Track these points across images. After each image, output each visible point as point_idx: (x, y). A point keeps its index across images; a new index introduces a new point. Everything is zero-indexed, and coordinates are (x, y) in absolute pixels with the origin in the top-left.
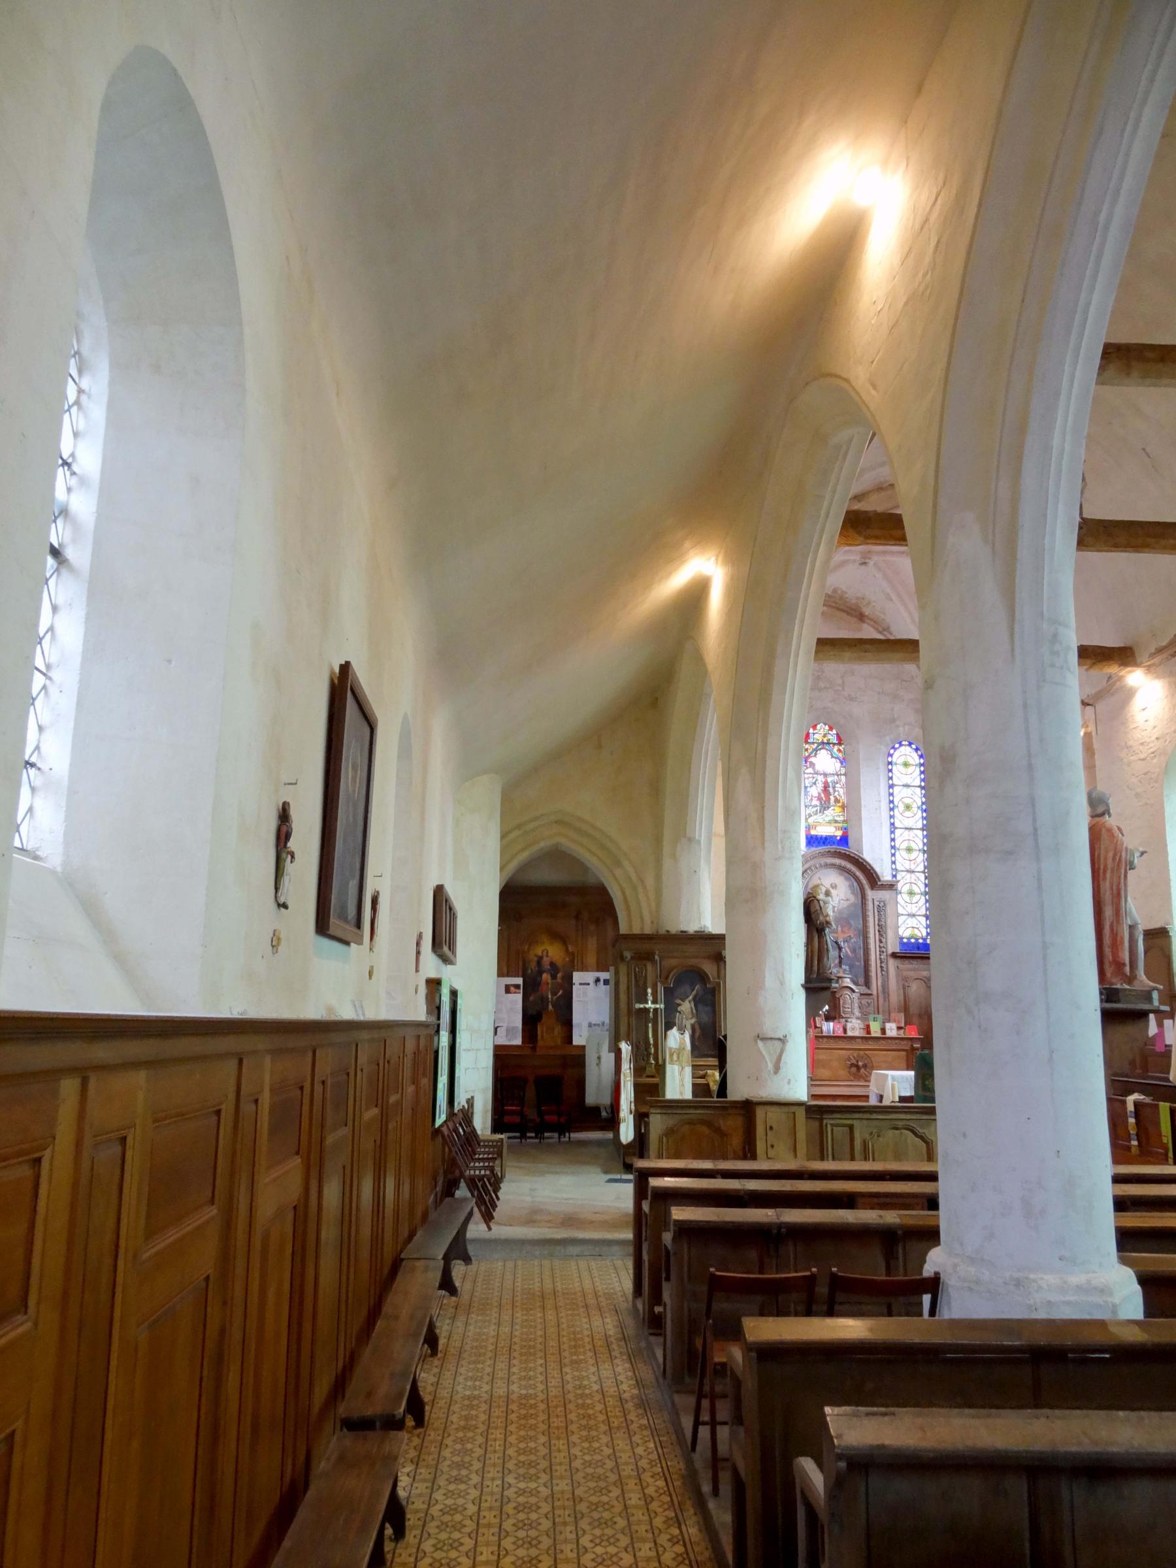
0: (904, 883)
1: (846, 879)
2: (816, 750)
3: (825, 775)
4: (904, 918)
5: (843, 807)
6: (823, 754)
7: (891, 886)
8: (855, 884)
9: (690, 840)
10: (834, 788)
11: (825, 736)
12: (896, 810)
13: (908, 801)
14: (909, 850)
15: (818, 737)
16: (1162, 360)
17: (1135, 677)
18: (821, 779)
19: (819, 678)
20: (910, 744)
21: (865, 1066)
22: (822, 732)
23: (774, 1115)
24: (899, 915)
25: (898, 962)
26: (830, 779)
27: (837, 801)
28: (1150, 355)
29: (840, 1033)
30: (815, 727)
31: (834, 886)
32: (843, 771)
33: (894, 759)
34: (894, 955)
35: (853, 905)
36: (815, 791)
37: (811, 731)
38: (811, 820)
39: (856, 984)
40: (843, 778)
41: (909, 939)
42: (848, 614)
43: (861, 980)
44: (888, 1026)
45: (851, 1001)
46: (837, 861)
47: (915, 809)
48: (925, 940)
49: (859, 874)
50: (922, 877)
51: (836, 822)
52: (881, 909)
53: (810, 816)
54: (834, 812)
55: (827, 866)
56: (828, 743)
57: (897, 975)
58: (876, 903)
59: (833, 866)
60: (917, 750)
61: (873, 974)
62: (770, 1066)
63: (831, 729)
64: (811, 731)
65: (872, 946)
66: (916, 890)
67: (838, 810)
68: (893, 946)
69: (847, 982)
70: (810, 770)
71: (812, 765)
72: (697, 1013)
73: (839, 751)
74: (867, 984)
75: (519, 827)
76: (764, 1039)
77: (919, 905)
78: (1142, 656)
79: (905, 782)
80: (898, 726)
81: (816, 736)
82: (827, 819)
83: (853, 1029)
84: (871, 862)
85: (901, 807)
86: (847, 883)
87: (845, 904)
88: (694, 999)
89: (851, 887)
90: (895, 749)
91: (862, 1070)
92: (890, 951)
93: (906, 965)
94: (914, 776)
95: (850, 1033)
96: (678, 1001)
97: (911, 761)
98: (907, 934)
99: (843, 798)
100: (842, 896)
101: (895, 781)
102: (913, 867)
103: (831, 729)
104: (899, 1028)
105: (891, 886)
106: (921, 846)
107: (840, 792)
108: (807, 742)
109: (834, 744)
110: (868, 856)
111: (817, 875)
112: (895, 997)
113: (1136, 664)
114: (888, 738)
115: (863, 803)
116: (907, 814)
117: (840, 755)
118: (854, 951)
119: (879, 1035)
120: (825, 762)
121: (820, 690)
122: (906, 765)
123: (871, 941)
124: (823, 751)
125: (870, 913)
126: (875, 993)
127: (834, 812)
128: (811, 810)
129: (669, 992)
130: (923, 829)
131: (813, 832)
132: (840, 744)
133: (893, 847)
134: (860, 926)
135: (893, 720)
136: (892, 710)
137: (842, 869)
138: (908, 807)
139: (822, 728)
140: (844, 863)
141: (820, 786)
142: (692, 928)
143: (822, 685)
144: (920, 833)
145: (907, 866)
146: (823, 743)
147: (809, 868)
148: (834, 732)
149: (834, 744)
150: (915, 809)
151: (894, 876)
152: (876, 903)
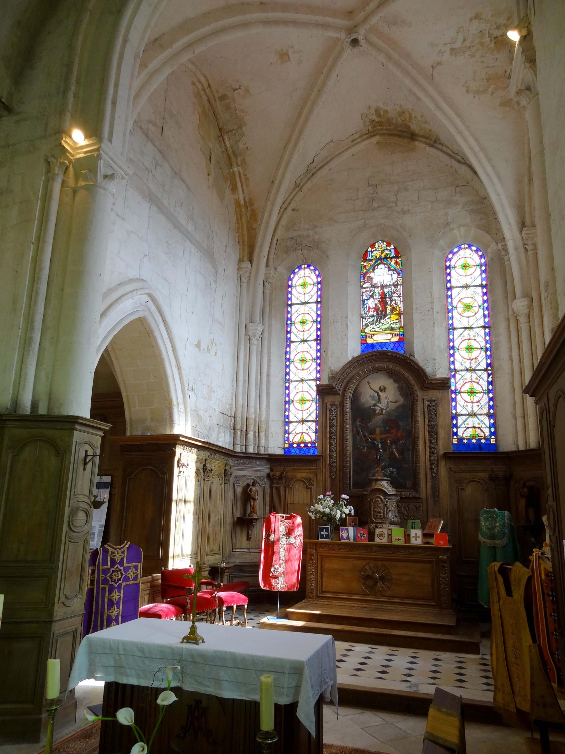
0: (462, 382)
1: (396, 381)
2: (374, 267)
3: (382, 287)
4: (464, 418)
5: (399, 314)
7: (444, 385)
8: (404, 385)
10: (391, 297)
11: (382, 253)
12: (455, 312)
13: (468, 301)
14: (470, 349)
15: (376, 254)
19: (373, 199)
20: (470, 247)
21: (382, 578)
22: (380, 249)
24: (455, 417)
26: (386, 291)
27: (393, 309)
29: (364, 539)
30: (373, 246)
32: (400, 281)
33: (453, 263)
34: (447, 456)
35: (403, 406)
36: (371, 303)
37: (370, 249)
38: (367, 330)
39: (393, 484)
40: (400, 288)
41: (469, 439)
42: (400, 136)
43: (409, 483)
44: (413, 533)
46: (386, 365)
47: (476, 309)
48: (488, 439)
50: (485, 375)
51: (392, 329)
52: (432, 408)
53: (367, 326)
55: (376, 370)
56: (386, 258)
58: (427, 403)
60: (477, 251)
64: (370, 249)
67: (394, 317)
71: (370, 279)
73: (397, 263)
74: (415, 486)
77: (482, 403)
79: (463, 283)
80: (452, 229)
81: (374, 253)
82: (384, 327)
83: (381, 535)
84: (421, 364)
85: (460, 308)
86: (396, 385)
87: (393, 406)
89: (400, 389)
90: (454, 254)
91: (380, 583)
92: (442, 451)
94: (476, 276)
95: (378, 540)
97: (470, 262)
98: (468, 434)
99: (401, 306)
100: (391, 398)
101: (454, 283)
102: (473, 366)
103: (389, 244)
104: (425, 536)
106: (483, 344)
107: (398, 301)
108: (365, 260)
109: (392, 258)
110: (419, 358)
112: (446, 501)
114: (442, 242)
115: (414, 307)
116: (468, 314)
117: (398, 267)
118: (401, 453)
119: (402, 543)
120: (382, 275)
121: (373, 209)
122: (465, 267)
124: (381, 266)
125: (420, 414)
126: (423, 496)
127: (391, 320)
130: (484, 327)
131: (369, 341)
132: (397, 257)
133: (453, 348)
135: (448, 224)
136: (446, 214)
137: (391, 374)
138: (468, 307)
141: (377, 297)
143: (375, 205)
144: (482, 332)
145: (467, 365)
146: (380, 258)
147: (358, 374)
148: (392, 247)
149: (392, 258)
150: (476, 309)
152: (427, 403)
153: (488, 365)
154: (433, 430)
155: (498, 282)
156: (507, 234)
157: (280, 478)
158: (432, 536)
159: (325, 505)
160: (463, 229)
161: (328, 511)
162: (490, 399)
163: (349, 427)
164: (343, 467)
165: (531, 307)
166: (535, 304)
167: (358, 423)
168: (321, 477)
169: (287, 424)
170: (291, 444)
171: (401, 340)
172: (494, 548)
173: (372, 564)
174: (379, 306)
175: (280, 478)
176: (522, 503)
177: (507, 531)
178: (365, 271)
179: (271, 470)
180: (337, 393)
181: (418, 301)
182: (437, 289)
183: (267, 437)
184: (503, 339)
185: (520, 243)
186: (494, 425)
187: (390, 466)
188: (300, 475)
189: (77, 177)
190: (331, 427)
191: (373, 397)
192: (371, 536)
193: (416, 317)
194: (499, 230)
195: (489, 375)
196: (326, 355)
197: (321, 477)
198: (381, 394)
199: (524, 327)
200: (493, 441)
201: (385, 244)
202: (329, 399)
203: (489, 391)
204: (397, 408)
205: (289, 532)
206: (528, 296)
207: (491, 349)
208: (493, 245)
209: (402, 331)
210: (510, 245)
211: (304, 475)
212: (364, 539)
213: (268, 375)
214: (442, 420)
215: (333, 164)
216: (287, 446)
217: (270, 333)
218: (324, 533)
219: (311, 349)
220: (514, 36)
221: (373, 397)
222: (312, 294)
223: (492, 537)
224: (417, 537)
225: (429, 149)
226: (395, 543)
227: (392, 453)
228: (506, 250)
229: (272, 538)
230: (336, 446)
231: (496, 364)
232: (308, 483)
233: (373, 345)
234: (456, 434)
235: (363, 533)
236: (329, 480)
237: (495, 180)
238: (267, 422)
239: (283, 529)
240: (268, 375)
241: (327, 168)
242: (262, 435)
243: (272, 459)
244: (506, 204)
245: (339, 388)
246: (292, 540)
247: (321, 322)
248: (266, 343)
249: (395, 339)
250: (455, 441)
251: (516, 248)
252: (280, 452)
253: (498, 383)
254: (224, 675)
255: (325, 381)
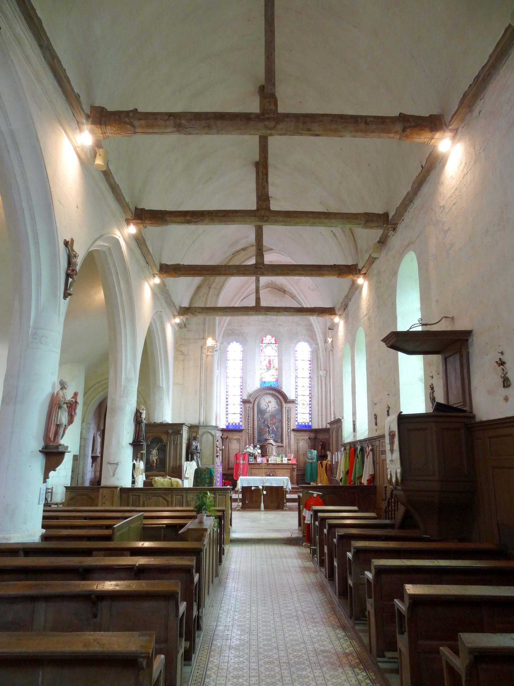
0: (300, 400)
1: (275, 399)
2: (266, 346)
3: (269, 356)
5: (276, 369)
6: (269, 348)
9: (159, 387)
16: (224, 216)
17: (336, 319)
18: (268, 359)
23: (105, 491)
24: (296, 414)
25: (296, 433)
26: (271, 358)
27: (274, 367)
28: (221, 215)
30: (266, 337)
31: (270, 402)
32: (277, 355)
34: (294, 430)
35: (277, 409)
37: (264, 338)
39: (276, 441)
40: (277, 358)
43: (279, 440)
45: (273, 449)
46: (271, 392)
48: (308, 423)
49: (280, 397)
52: (289, 411)
54: (273, 372)
55: (267, 394)
57: (295, 438)
59: (269, 394)
61: (284, 438)
62: (111, 473)
63: (272, 337)
65: (284, 426)
66: (305, 403)
68: (293, 426)
69: (272, 441)
70: (263, 355)
72: (158, 454)
74: (282, 442)
75: (99, 383)
76: (110, 464)
78: (337, 312)
84: (285, 392)
88: (158, 449)
89: (277, 402)
92: (292, 429)
93: (299, 434)
95: (270, 462)
96: (152, 450)
99: (276, 366)
103: (272, 337)
104: (288, 460)
105: (293, 402)
107: (276, 364)
108: (262, 343)
110: (285, 390)
111: (263, 397)
112: (293, 447)
113: (335, 314)
114: (294, 341)
117: (276, 348)
118: (277, 428)
119: (280, 462)
123: (284, 424)
126: (285, 445)
127: (273, 372)
128: (263, 371)
129: (148, 446)
131: (264, 380)
132: (276, 344)
134: (280, 418)
135: (297, 334)
139: (269, 337)
140: (274, 392)
141: (267, 361)
142: (159, 421)
147: (260, 395)
148: (274, 338)
151: (296, 397)
153: (310, 394)
154: (289, 420)
155: (315, 360)
156: (320, 345)
157: (227, 438)
158: (290, 460)
159: (250, 449)
160: (303, 336)
161: (252, 452)
162: (310, 407)
163: (256, 417)
164: (253, 434)
165: (326, 374)
166: (328, 373)
167: (259, 416)
168: (244, 438)
169: (227, 414)
170: (229, 424)
171: (277, 381)
172: (311, 463)
173: (269, 470)
174: (268, 365)
175: (227, 438)
176: (320, 447)
177: (315, 457)
178: (262, 348)
179: (223, 435)
180: (251, 403)
181: (285, 366)
182: (292, 361)
183: (220, 420)
184: (316, 383)
185: (324, 349)
186: (311, 418)
187: (272, 433)
188: (235, 437)
189: (208, 350)
190: (248, 417)
191: (266, 405)
192: (268, 461)
193: (284, 372)
194: (316, 339)
195: (310, 398)
196: (246, 385)
197: (244, 438)
198: (269, 404)
199: (323, 382)
200: (310, 424)
201: (271, 337)
202: (248, 405)
203: (310, 404)
204: (276, 410)
205: (244, 459)
206: (325, 370)
207: (311, 387)
208: (314, 345)
209: (277, 377)
210: (320, 348)
211: (237, 437)
212: (265, 462)
213: (220, 393)
214: (293, 416)
215: (249, 297)
216: (227, 424)
217: (220, 373)
218: (251, 460)
219: (238, 382)
220: (330, 340)
221: (266, 405)
222: (240, 356)
223: (312, 459)
224: (285, 460)
225: (292, 299)
226: (277, 463)
227: (273, 428)
228: (318, 349)
229: (238, 461)
230: (251, 425)
231: (313, 394)
232: (238, 440)
233: (265, 382)
234: (297, 421)
235: (264, 460)
236: (247, 439)
237: (317, 323)
238: (220, 414)
239: (241, 458)
240: (220, 393)
241: (247, 299)
242: (218, 420)
243: (223, 430)
244: (320, 333)
245: (252, 400)
246: (245, 462)
247: (244, 370)
248: (219, 379)
249: (275, 380)
250: (297, 424)
251: (322, 350)
252: (225, 427)
253: (313, 401)
254: (273, 482)
255: (245, 397)
